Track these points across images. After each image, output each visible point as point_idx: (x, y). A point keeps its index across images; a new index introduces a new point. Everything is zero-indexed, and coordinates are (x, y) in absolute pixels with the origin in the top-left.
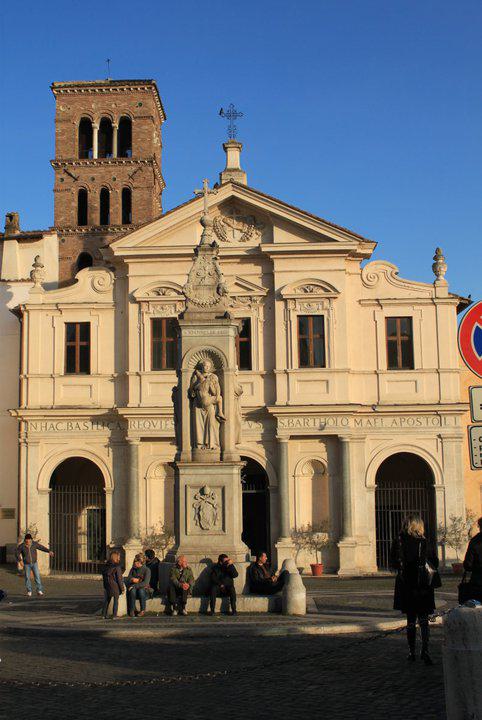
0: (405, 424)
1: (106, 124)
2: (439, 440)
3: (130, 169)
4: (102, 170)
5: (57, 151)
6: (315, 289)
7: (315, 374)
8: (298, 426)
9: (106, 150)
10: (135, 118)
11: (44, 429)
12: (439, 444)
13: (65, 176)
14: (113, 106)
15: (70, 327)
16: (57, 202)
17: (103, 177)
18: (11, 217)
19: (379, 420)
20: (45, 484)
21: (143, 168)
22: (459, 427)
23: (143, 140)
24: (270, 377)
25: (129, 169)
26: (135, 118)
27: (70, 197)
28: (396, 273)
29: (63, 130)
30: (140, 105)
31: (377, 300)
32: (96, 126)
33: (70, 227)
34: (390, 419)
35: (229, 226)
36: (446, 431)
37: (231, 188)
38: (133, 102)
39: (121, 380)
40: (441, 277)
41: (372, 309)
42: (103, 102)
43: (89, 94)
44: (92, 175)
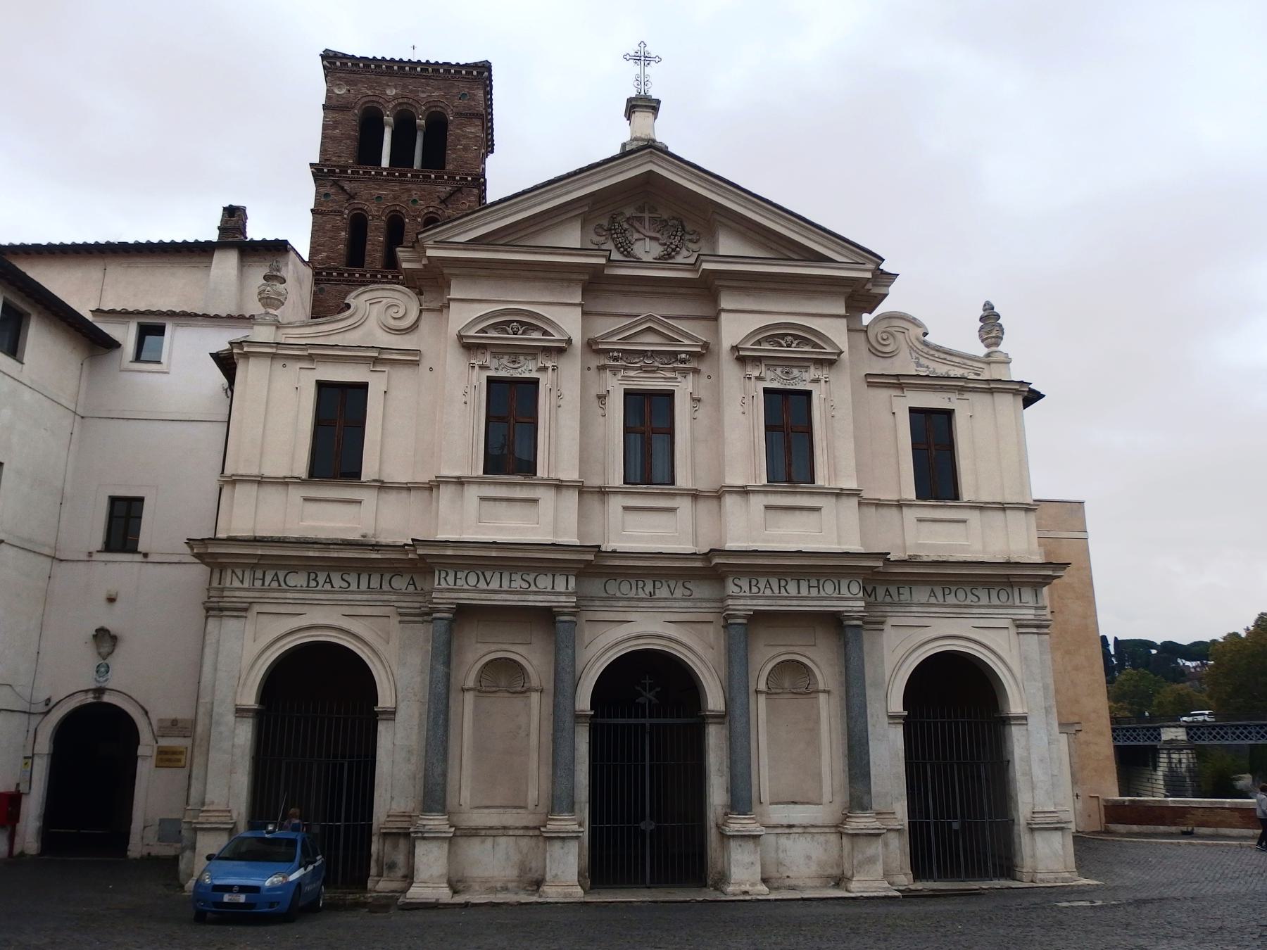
0: (951, 599)
2: (1013, 630)
8: (768, 592)
11: (258, 583)
17: (395, 198)
19: (905, 591)
20: (250, 699)
23: (466, 148)
25: (440, 188)
27: (340, 224)
33: (335, 269)
34: (929, 589)
35: (639, 232)
41: (884, 394)
42: (405, 86)
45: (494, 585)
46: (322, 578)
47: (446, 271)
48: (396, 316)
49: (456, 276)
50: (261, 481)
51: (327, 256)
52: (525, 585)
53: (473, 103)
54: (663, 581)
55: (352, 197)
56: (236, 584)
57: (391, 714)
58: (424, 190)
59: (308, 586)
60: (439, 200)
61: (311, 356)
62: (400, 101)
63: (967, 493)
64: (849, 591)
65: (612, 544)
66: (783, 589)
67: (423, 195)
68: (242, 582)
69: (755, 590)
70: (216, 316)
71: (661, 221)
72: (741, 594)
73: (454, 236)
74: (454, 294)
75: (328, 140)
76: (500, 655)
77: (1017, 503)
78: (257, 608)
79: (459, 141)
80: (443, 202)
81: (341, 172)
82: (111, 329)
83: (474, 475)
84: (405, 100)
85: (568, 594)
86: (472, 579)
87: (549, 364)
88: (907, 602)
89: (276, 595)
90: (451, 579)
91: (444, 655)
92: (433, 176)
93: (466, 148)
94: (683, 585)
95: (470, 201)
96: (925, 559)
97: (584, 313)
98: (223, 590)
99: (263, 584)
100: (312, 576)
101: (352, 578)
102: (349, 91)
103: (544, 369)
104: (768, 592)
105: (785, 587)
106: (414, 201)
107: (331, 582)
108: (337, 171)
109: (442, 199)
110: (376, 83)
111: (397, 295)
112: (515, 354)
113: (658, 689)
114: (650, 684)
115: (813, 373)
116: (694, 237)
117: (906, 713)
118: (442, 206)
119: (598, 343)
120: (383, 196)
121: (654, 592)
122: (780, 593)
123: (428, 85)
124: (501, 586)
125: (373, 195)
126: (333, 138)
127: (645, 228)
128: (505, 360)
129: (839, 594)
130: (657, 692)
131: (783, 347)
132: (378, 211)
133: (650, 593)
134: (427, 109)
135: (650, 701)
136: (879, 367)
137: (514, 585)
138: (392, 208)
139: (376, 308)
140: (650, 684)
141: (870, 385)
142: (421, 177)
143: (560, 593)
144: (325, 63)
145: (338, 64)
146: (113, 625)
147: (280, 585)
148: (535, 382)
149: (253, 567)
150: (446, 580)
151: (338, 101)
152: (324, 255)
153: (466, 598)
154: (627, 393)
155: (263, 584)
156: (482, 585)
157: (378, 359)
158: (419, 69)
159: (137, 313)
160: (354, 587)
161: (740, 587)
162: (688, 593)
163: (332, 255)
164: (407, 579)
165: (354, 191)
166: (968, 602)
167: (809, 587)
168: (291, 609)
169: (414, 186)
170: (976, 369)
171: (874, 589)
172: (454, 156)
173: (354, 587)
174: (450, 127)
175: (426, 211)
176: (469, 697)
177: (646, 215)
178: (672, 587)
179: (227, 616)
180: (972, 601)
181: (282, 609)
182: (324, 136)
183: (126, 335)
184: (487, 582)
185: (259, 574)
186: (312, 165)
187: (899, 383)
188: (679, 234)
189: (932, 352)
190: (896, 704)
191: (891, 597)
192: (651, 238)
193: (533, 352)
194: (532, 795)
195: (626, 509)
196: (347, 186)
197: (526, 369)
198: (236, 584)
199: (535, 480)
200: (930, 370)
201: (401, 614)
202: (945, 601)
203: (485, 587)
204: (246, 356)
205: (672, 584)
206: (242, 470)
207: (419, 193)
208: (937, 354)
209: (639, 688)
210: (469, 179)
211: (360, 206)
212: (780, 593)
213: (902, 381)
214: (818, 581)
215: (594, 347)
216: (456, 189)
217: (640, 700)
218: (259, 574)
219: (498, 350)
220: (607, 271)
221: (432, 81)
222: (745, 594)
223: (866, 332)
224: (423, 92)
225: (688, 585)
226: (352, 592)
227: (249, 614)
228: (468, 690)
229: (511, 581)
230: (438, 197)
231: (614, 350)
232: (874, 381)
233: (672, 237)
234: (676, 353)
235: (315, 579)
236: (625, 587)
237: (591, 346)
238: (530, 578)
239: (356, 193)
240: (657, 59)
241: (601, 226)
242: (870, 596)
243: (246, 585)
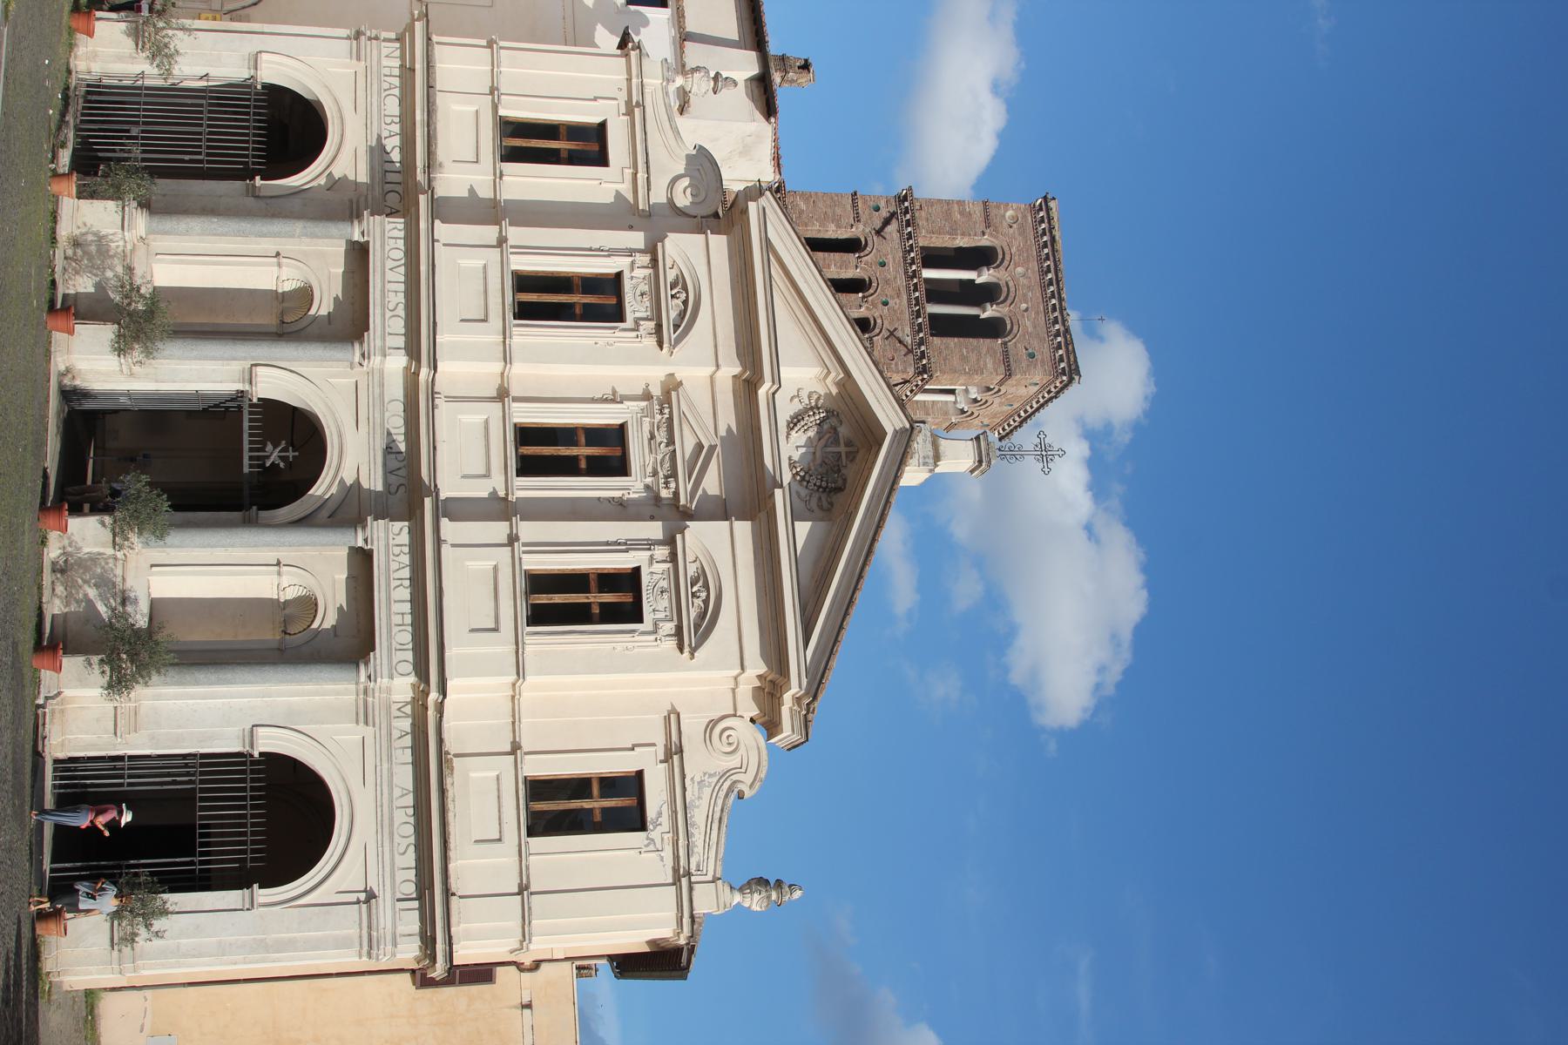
1: (989, 293)
4: (901, 281)
5: (931, 203)
6: (698, 602)
7: (511, 607)
9: (937, 292)
10: (1005, 344)
11: (387, 71)
12: (353, 897)
13: (884, 213)
14: (1024, 306)
16: (834, 199)
17: (887, 282)
18: (806, 66)
21: (910, 357)
22: (395, 944)
23: (964, 359)
24: (501, 508)
25: (908, 330)
26: (1005, 344)
28: (741, 796)
30: (1032, 356)
31: (680, 751)
32: (983, 277)
36: (384, 905)
37: (899, 426)
38: (1035, 343)
39: (491, 211)
40: (737, 898)
41: (660, 741)
43: (1040, 261)
44: (890, 260)
45: (390, 276)
51: (801, 212)
52: (391, 307)
53: (1024, 365)
54: (405, 462)
55: (879, 232)
56: (385, 52)
58: (902, 313)
59: (385, 116)
62: (1011, 284)
63: (538, 843)
64: (400, 662)
66: (399, 582)
67: (895, 311)
68: (386, 56)
69: (397, 550)
71: (838, 466)
72: (391, 536)
73: (772, 224)
75: (945, 207)
77: (530, 908)
79: (973, 351)
80: (892, 334)
84: (1012, 289)
88: (394, 758)
89: (375, 87)
92: (920, 320)
94: (401, 485)
95: (896, 365)
96: (448, 781)
99: (386, 76)
102: (1011, 227)
104: (394, 566)
105: (401, 585)
107: (390, 136)
108: (908, 217)
110: (1028, 257)
113: (282, 465)
114: (288, 456)
115: (669, 627)
116: (825, 504)
117: (256, 755)
118: (885, 333)
120: (886, 267)
121: (391, 453)
122: (394, 579)
123: (1037, 313)
124: (389, 282)
125: (886, 255)
126: (948, 215)
127: (825, 446)
129: (396, 650)
130: (279, 464)
131: (692, 588)
133: (391, 448)
135: (268, 457)
136: (692, 726)
137: (392, 295)
138: (873, 279)
140: (288, 456)
141: (667, 719)
142: (918, 308)
143: (384, 340)
147: (385, 90)
150: (394, 229)
151: (996, 215)
152: (803, 207)
155: (386, 76)
156: (390, 264)
161: (399, 534)
162: (393, 490)
163: (804, 216)
165: (885, 235)
166: (397, 839)
167: (403, 614)
168: (361, 100)
169: (905, 301)
170: (705, 864)
171: (407, 716)
172: (952, 345)
174: (988, 341)
177: (842, 449)
178: (399, 472)
180: (399, 844)
181: (361, 93)
182: (948, 202)
184: (395, 267)
186: (910, 189)
187: (674, 752)
188: (824, 479)
189: (720, 802)
190: (270, 742)
191: (400, 738)
192: (814, 453)
196: (892, 228)
197: (635, 306)
199: (509, 318)
200: (696, 801)
202: (397, 808)
205: (402, 472)
207: (896, 307)
208: (718, 809)
211: (870, 243)
212: (394, 579)
213: (675, 756)
214: (408, 625)
216: (910, 347)
217: (269, 447)
221: (1043, 318)
222: (391, 538)
223: (735, 715)
225: (402, 489)
227: (354, 61)
229: (396, 292)
230: (896, 329)
231: (671, 407)
232: (672, 718)
233: (819, 477)
234: (673, 474)
235: (393, 122)
238: (401, 311)
239: (885, 239)
240: (1046, 470)
242: (399, 709)
243: (385, 62)
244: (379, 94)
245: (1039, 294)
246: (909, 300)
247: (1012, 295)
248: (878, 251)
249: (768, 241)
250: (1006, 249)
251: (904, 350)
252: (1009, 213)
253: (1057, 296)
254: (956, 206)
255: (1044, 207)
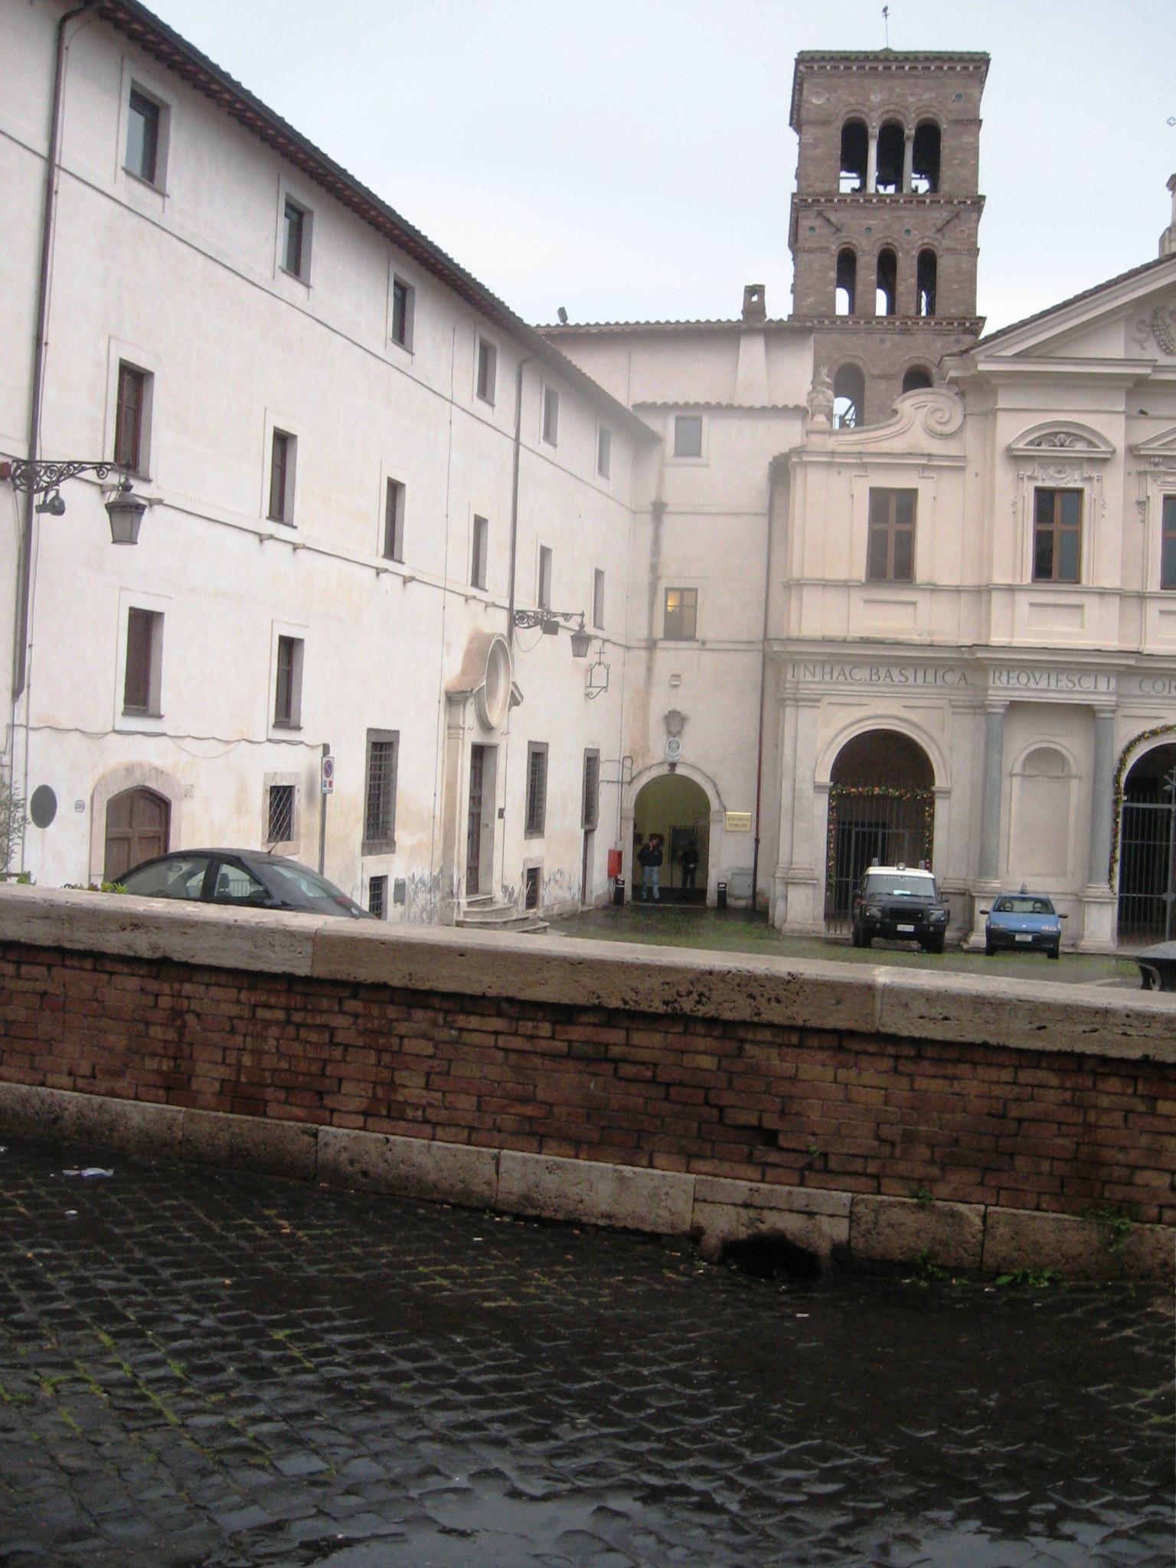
3: (939, 216)
4: (887, 215)
11: (827, 677)
13: (817, 223)
15: (880, 498)
17: (887, 228)
20: (825, 777)
21: (963, 215)
23: (963, 163)
25: (936, 214)
29: (816, 139)
45: (1043, 684)
46: (883, 673)
47: (994, 381)
48: (944, 420)
49: (1002, 385)
50: (825, 584)
52: (1071, 685)
57: (947, 793)
60: (934, 229)
61: (862, 463)
62: (887, 108)
65: (1149, 648)
68: (814, 676)
70: (751, 409)
74: (1000, 405)
76: (1045, 745)
78: (827, 699)
81: (827, 201)
82: (654, 424)
83: (1025, 583)
84: (892, 107)
85: (1110, 694)
86: (1023, 679)
87: (1094, 475)
90: (1004, 678)
91: (992, 746)
92: (928, 201)
93: (963, 163)
95: (970, 229)
97: (1126, 417)
98: (798, 683)
100: (874, 671)
101: (910, 673)
103: (1090, 479)
106: (908, 231)
108: (823, 200)
109: (939, 226)
111: (941, 399)
112: (1062, 464)
118: (939, 236)
119: (1140, 449)
128: (1051, 471)
132: (868, 245)
134: (917, 116)
137: (1060, 684)
138: (884, 241)
139: (923, 411)
144: (801, 68)
145: (816, 68)
146: (683, 708)
148: (1079, 492)
149: (823, 663)
152: (811, 300)
153: (1017, 696)
154: (1167, 498)
156: (1032, 685)
157: (928, 464)
158: (907, 68)
159: (676, 406)
160: (911, 681)
164: (958, 674)
173: (911, 681)
175: (920, 243)
176: (1016, 781)
179: (806, 706)
181: (850, 700)
183: (667, 429)
185: (827, 669)
193: (1077, 462)
194: (1070, 867)
195: (1162, 612)
196: (833, 217)
197: (1071, 480)
198: (809, 678)
201: (954, 707)
203: (1034, 686)
204: (805, 464)
206: (808, 574)
209: (1166, 777)
210: (969, 202)
211: (848, 240)
215: (1135, 453)
217: (1168, 787)
218: (827, 669)
219: (1045, 461)
220: (1151, 378)
224: (912, 95)
226: (911, 686)
227: (820, 704)
228: (1015, 775)
230: (934, 225)
236: (1159, 686)
237: (1132, 451)
238: (1075, 679)
241: (1142, 322)
244: (852, 684)
245: (898, 82)
246: (905, 209)
247: (898, 108)
248: (855, 233)
249: (1015, 355)
250: (849, 108)
251: (956, 221)
252: (815, 101)
253: (901, 64)
254: (809, 152)
255: (809, 65)
